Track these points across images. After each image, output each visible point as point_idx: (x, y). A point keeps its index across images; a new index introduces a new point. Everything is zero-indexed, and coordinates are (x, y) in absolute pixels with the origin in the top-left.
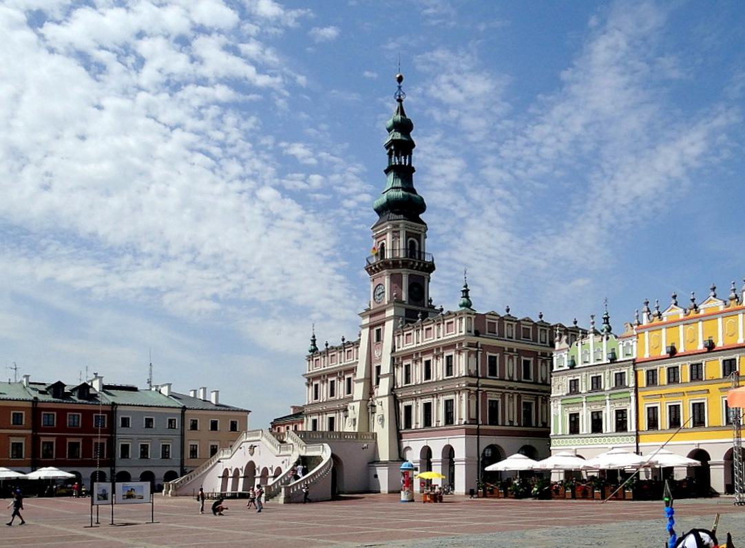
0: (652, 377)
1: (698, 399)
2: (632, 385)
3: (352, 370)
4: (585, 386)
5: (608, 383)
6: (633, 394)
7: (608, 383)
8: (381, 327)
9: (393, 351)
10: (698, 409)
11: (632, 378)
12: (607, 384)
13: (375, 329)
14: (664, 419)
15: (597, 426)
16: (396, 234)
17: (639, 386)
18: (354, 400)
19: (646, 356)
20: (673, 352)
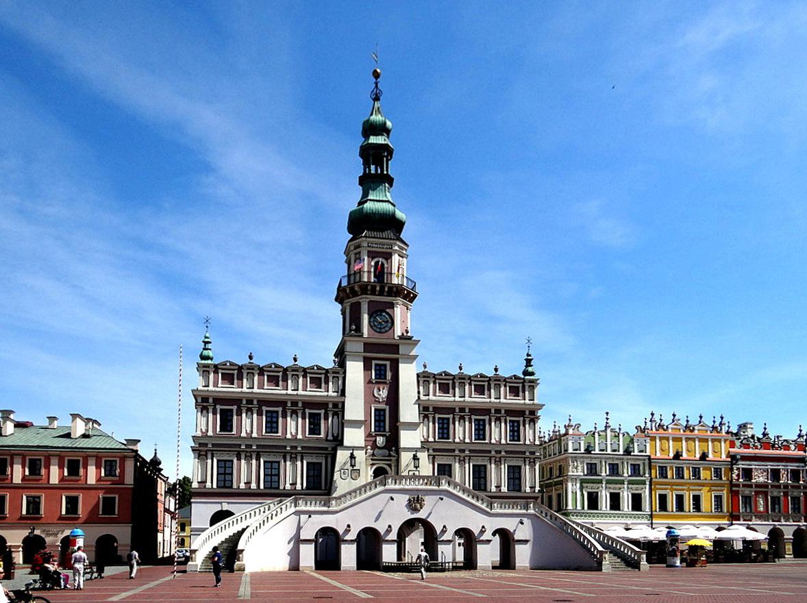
0: (663, 474)
1: (697, 493)
2: (647, 475)
3: (338, 408)
4: (604, 472)
5: (626, 472)
6: (648, 483)
7: (626, 472)
8: (388, 363)
9: (419, 397)
10: (697, 499)
11: (647, 472)
12: (625, 471)
13: (374, 362)
14: (672, 503)
15: (615, 502)
16: (401, 259)
17: (653, 476)
18: (346, 443)
19: (658, 455)
20: (677, 456)
